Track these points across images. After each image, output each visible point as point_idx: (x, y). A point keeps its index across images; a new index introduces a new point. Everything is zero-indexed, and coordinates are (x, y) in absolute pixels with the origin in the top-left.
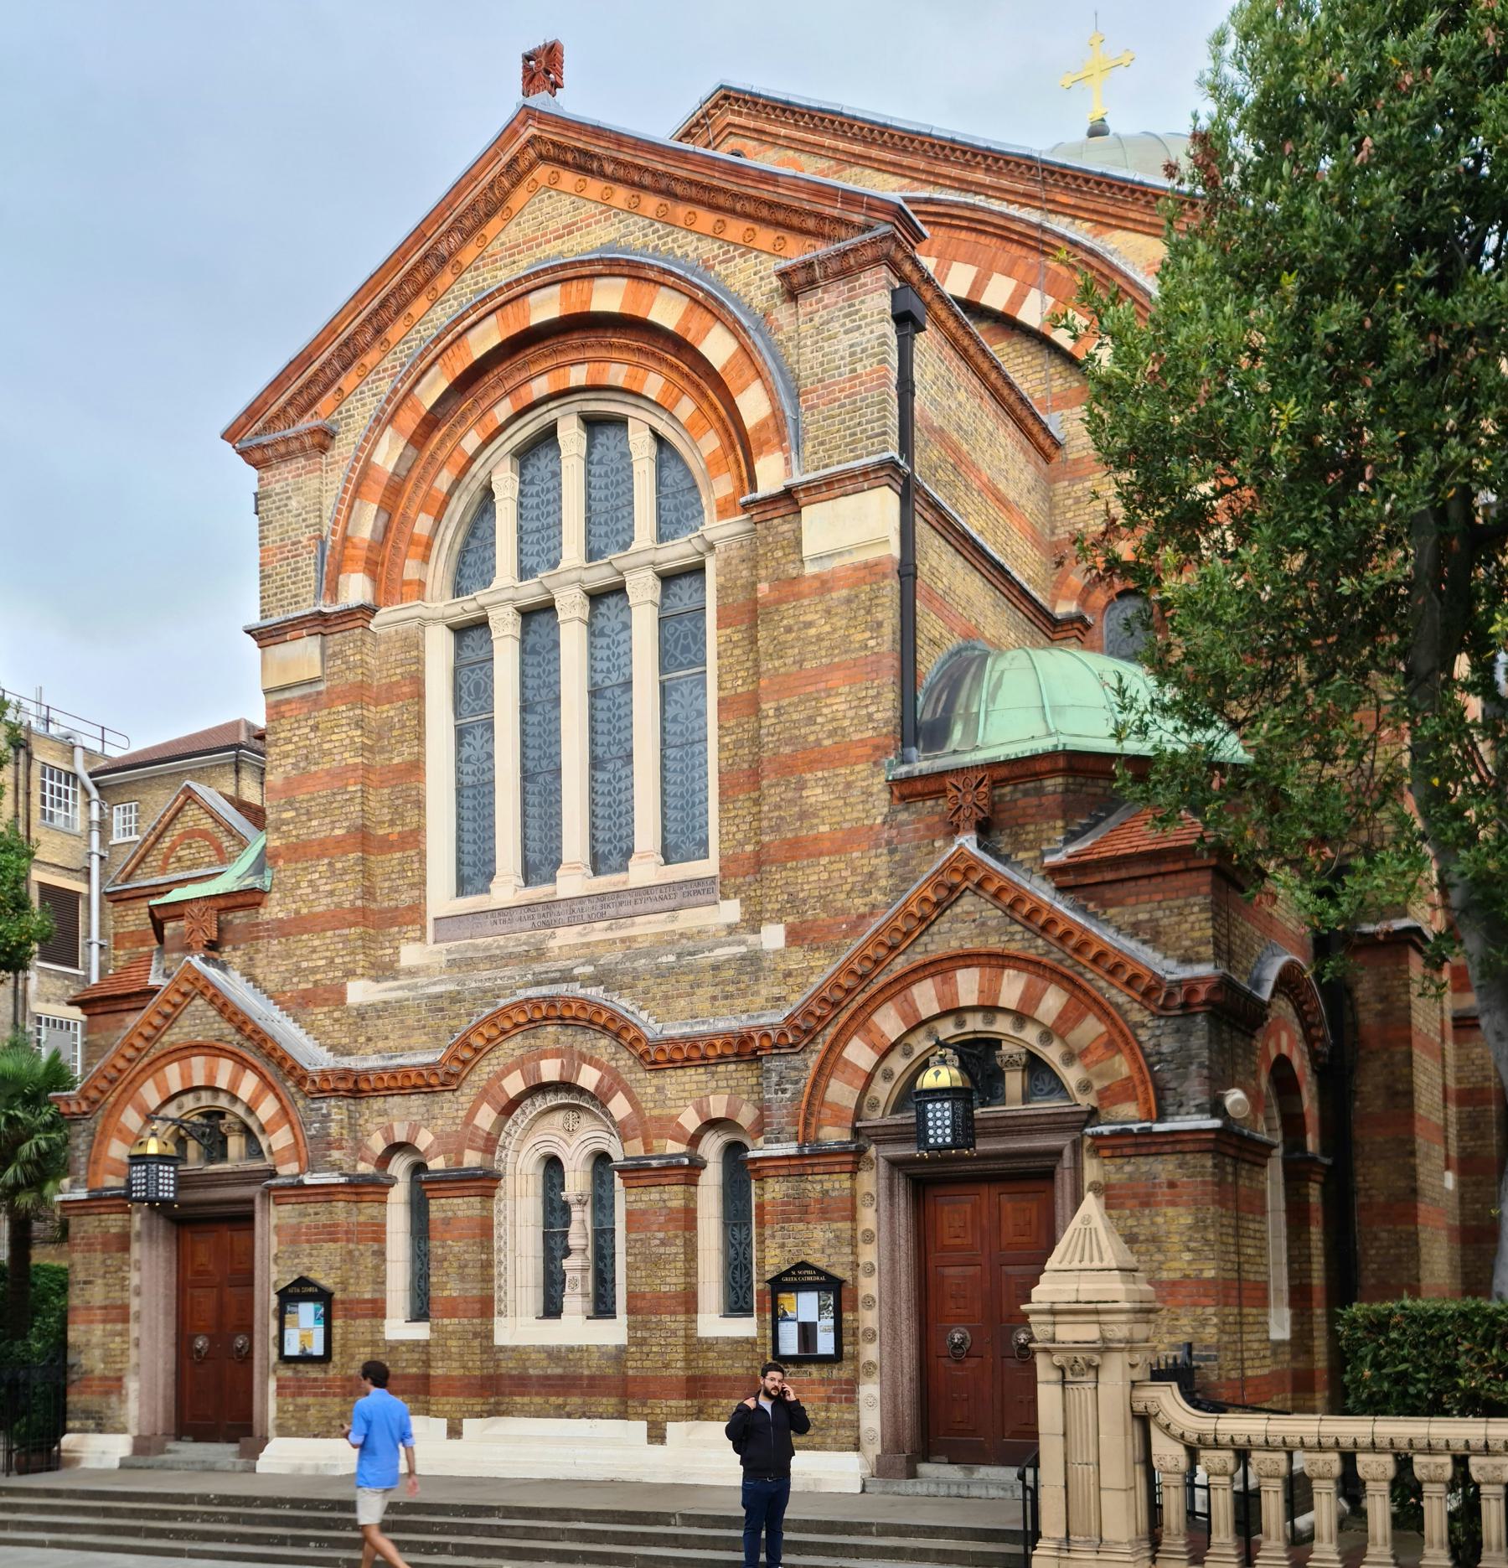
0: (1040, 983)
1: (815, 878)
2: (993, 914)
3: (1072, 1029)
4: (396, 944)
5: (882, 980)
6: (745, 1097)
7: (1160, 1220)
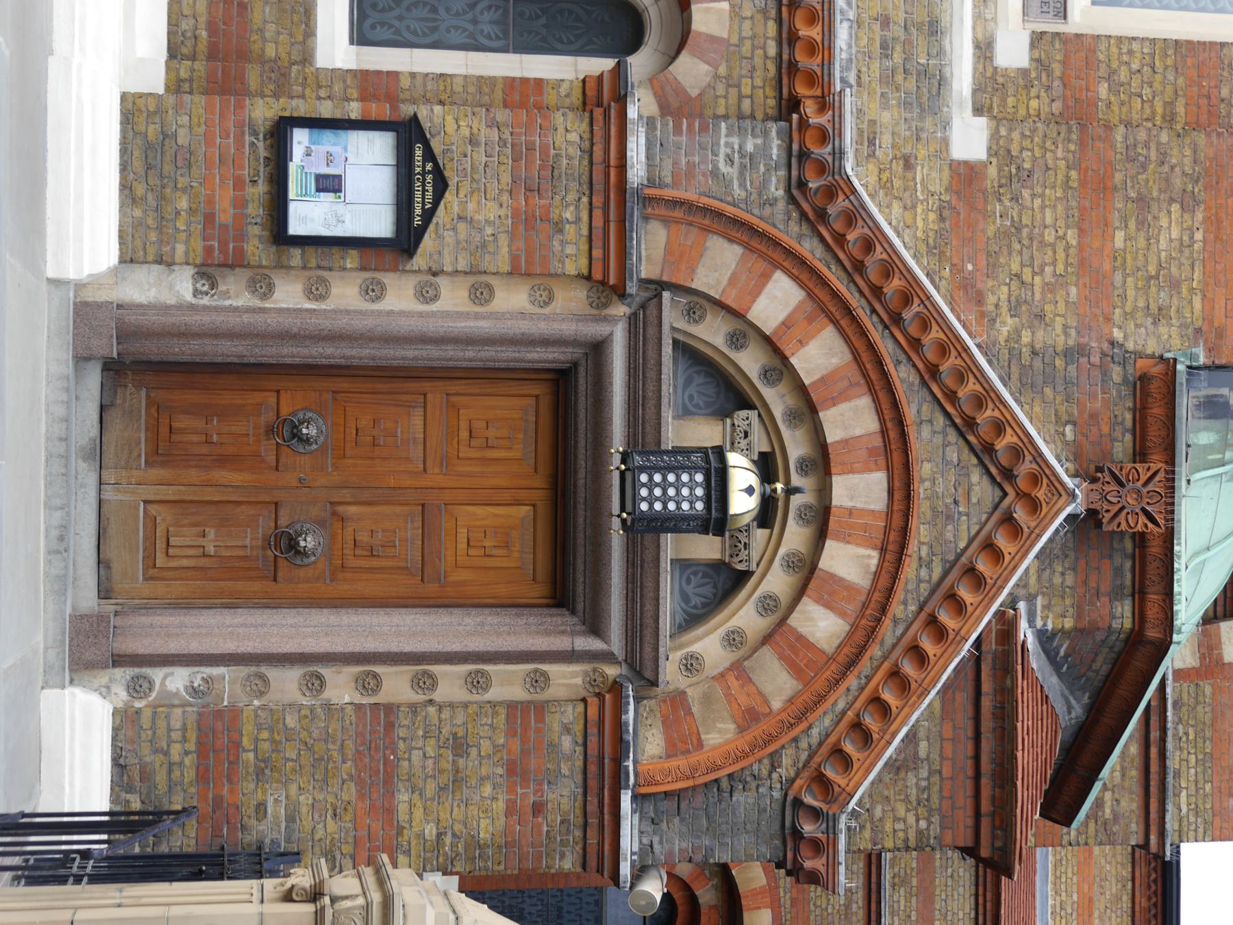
0: (852, 608)
1: (1049, 221)
2: (960, 534)
3: (782, 657)
5: (886, 347)
6: (722, 70)
7: (487, 790)
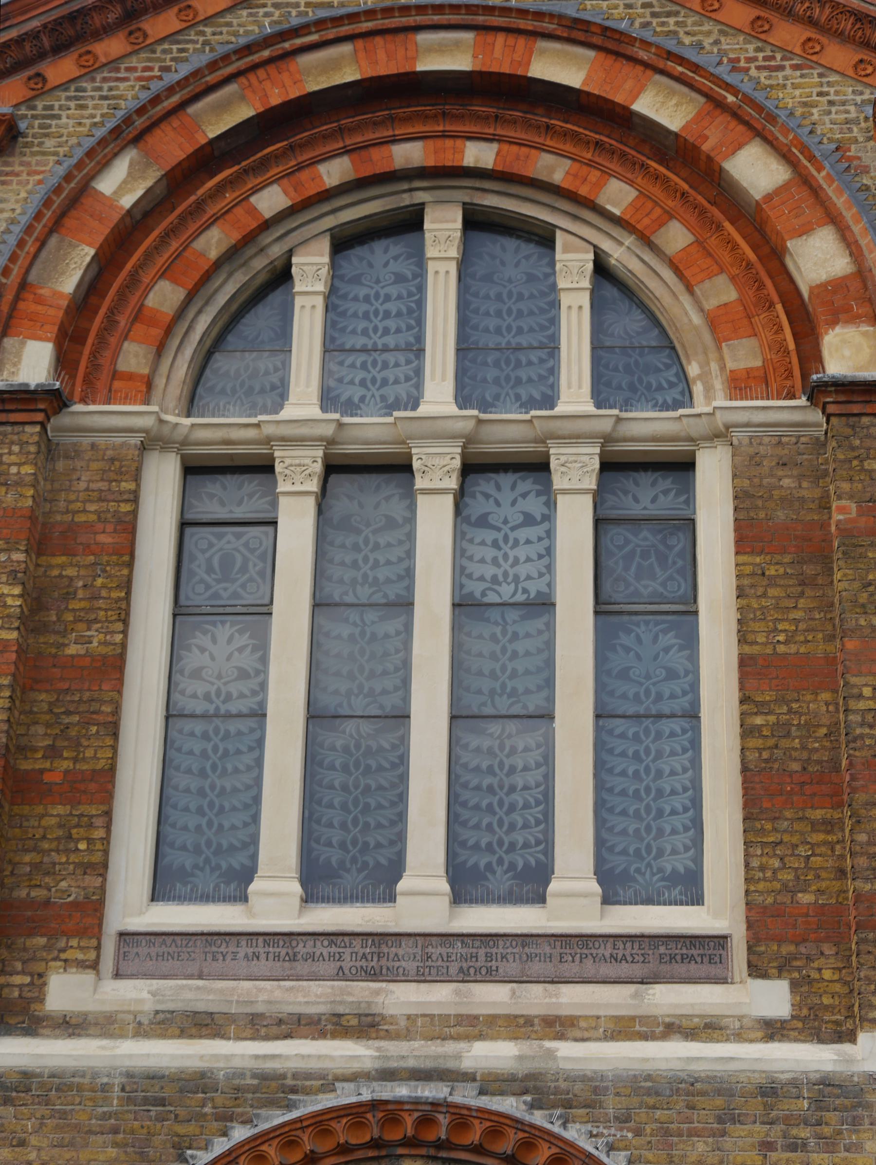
4: (39, 967)
